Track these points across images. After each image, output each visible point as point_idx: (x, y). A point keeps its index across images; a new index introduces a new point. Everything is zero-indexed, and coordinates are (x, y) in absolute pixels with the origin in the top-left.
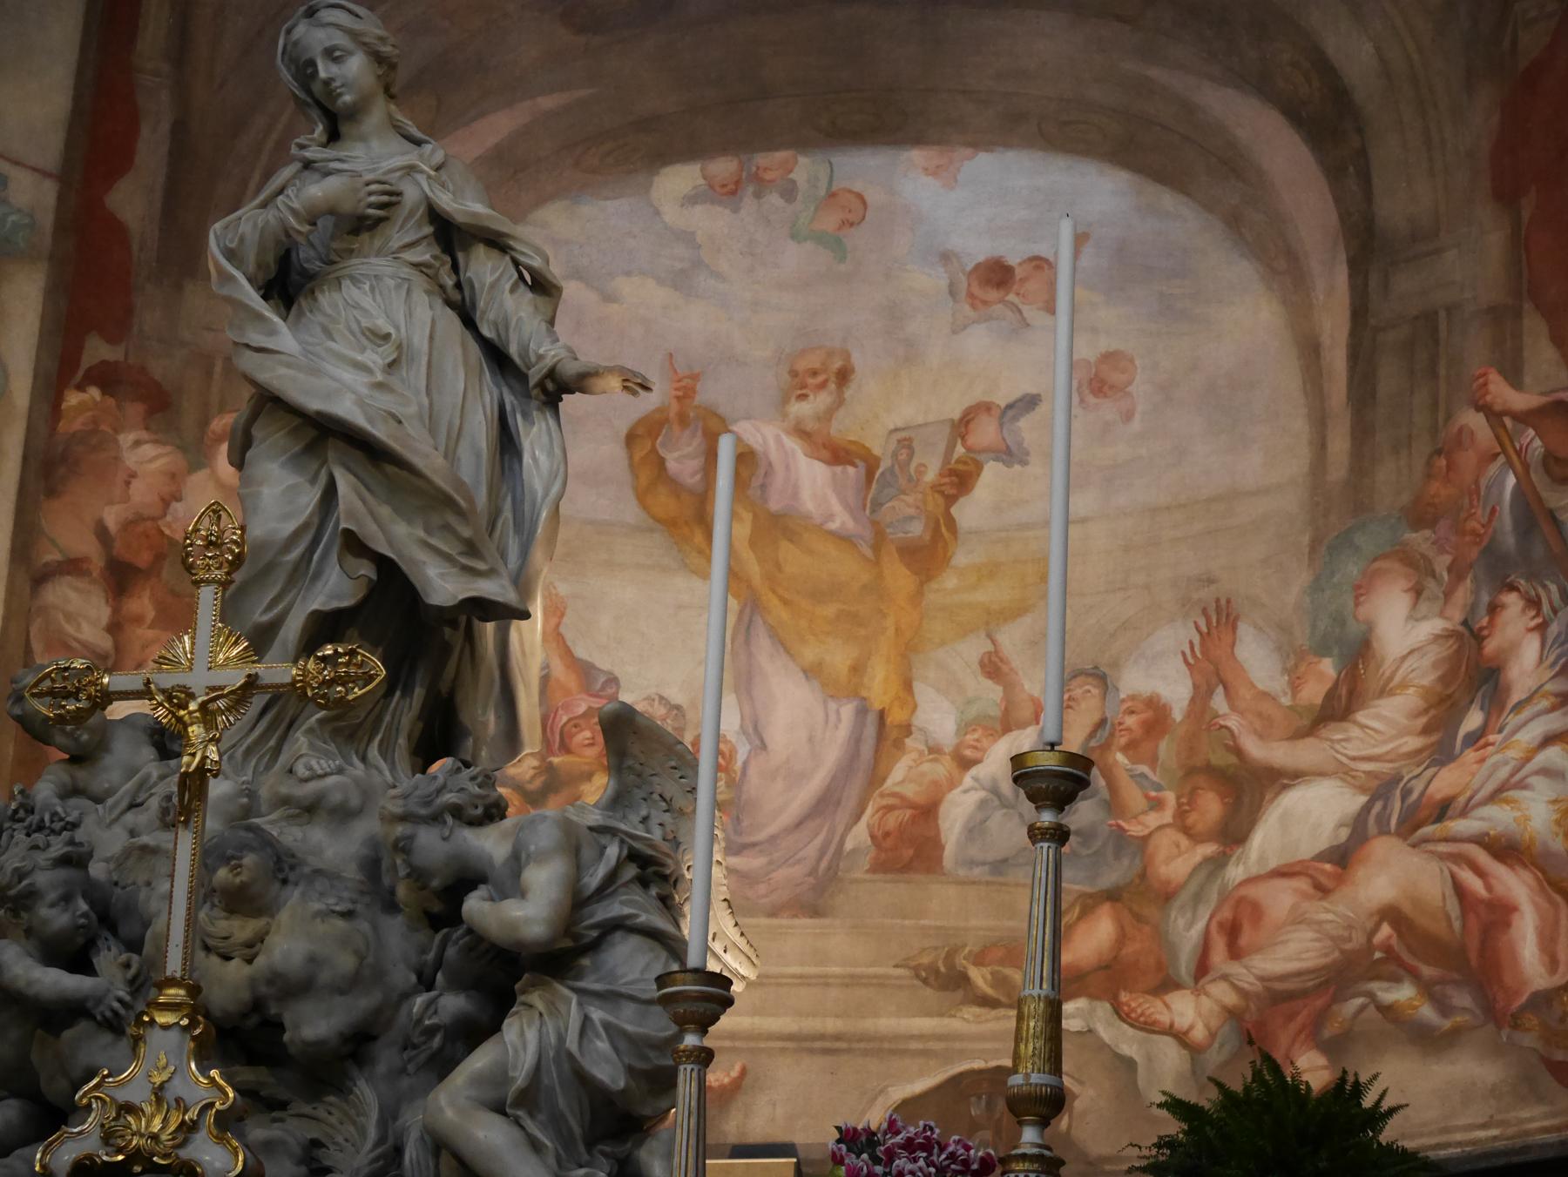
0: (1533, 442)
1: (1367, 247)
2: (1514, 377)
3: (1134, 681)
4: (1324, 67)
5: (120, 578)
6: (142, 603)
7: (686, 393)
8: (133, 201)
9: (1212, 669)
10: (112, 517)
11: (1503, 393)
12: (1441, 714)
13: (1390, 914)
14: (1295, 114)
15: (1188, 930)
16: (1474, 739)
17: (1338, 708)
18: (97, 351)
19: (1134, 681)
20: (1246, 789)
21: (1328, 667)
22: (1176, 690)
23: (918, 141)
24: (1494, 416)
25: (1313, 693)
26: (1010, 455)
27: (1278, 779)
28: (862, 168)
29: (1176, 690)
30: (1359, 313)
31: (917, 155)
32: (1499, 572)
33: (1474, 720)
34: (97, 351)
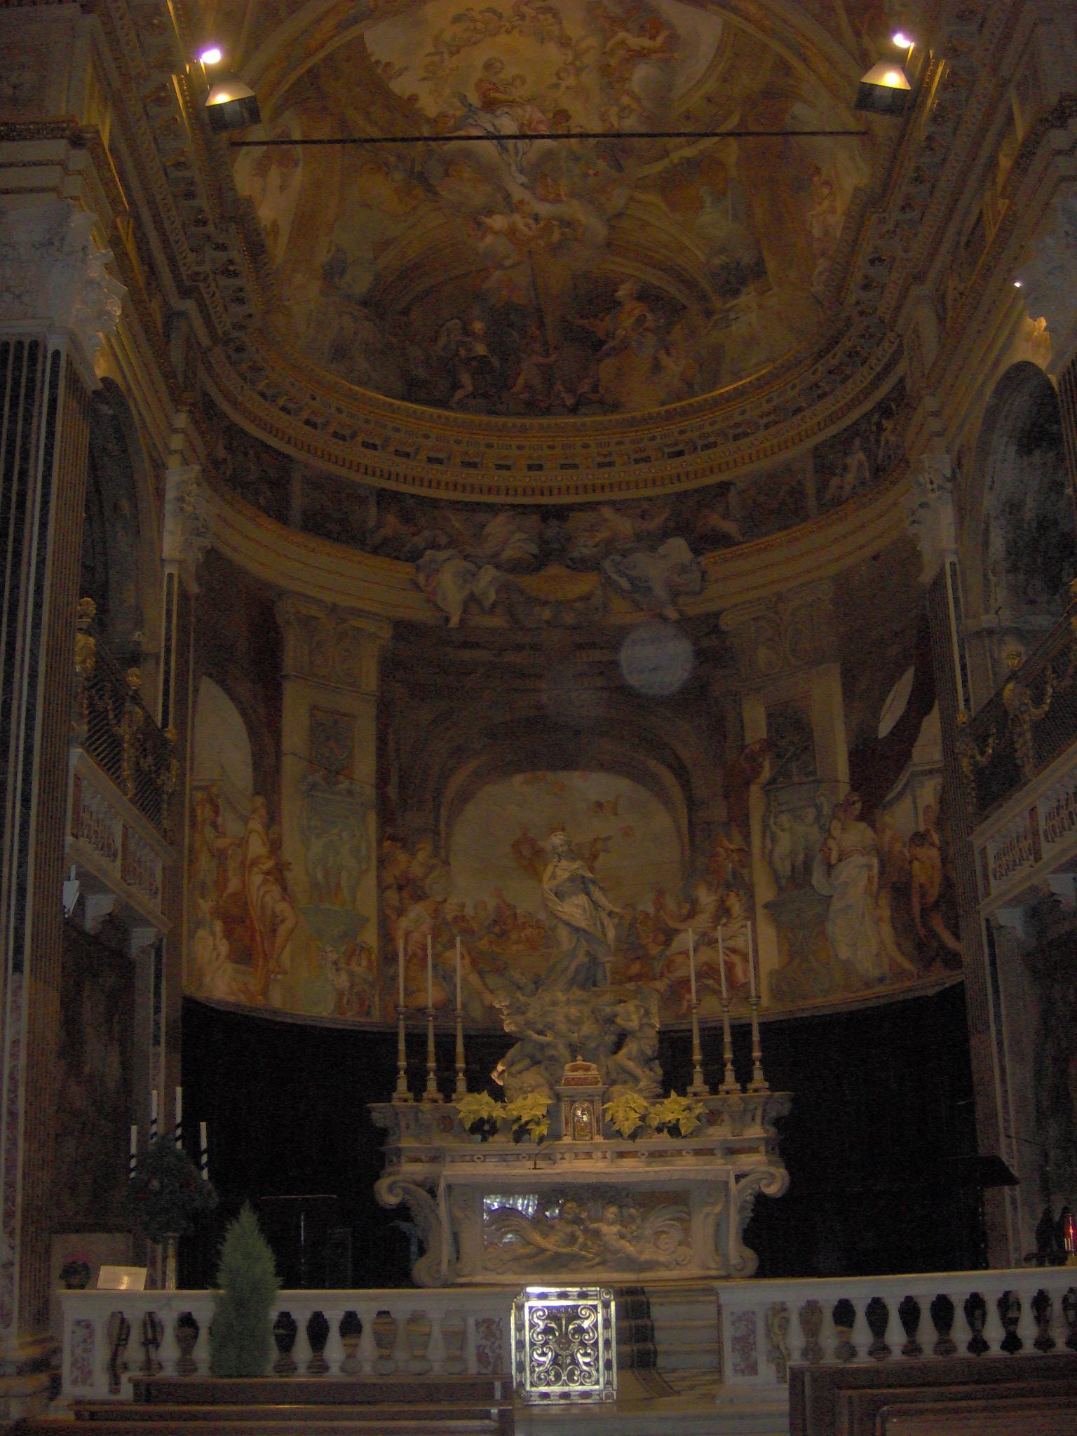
0: (735, 857)
1: (692, 804)
2: (730, 841)
3: (641, 907)
4: (677, 757)
5: (401, 888)
6: (405, 894)
7: (525, 835)
8: (392, 791)
9: (659, 906)
10: (397, 873)
11: (726, 843)
12: (716, 919)
13: (706, 963)
14: (670, 766)
15: (658, 966)
16: (724, 925)
17: (691, 915)
18: (390, 830)
19: (641, 907)
20: (670, 935)
21: (688, 906)
22: (651, 910)
23: (575, 769)
24: (726, 850)
25: (684, 911)
26: (607, 851)
27: (677, 931)
28: (563, 776)
29: (651, 910)
30: (690, 821)
31: (577, 773)
32: (728, 886)
33: (724, 920)
34: (390, 830)
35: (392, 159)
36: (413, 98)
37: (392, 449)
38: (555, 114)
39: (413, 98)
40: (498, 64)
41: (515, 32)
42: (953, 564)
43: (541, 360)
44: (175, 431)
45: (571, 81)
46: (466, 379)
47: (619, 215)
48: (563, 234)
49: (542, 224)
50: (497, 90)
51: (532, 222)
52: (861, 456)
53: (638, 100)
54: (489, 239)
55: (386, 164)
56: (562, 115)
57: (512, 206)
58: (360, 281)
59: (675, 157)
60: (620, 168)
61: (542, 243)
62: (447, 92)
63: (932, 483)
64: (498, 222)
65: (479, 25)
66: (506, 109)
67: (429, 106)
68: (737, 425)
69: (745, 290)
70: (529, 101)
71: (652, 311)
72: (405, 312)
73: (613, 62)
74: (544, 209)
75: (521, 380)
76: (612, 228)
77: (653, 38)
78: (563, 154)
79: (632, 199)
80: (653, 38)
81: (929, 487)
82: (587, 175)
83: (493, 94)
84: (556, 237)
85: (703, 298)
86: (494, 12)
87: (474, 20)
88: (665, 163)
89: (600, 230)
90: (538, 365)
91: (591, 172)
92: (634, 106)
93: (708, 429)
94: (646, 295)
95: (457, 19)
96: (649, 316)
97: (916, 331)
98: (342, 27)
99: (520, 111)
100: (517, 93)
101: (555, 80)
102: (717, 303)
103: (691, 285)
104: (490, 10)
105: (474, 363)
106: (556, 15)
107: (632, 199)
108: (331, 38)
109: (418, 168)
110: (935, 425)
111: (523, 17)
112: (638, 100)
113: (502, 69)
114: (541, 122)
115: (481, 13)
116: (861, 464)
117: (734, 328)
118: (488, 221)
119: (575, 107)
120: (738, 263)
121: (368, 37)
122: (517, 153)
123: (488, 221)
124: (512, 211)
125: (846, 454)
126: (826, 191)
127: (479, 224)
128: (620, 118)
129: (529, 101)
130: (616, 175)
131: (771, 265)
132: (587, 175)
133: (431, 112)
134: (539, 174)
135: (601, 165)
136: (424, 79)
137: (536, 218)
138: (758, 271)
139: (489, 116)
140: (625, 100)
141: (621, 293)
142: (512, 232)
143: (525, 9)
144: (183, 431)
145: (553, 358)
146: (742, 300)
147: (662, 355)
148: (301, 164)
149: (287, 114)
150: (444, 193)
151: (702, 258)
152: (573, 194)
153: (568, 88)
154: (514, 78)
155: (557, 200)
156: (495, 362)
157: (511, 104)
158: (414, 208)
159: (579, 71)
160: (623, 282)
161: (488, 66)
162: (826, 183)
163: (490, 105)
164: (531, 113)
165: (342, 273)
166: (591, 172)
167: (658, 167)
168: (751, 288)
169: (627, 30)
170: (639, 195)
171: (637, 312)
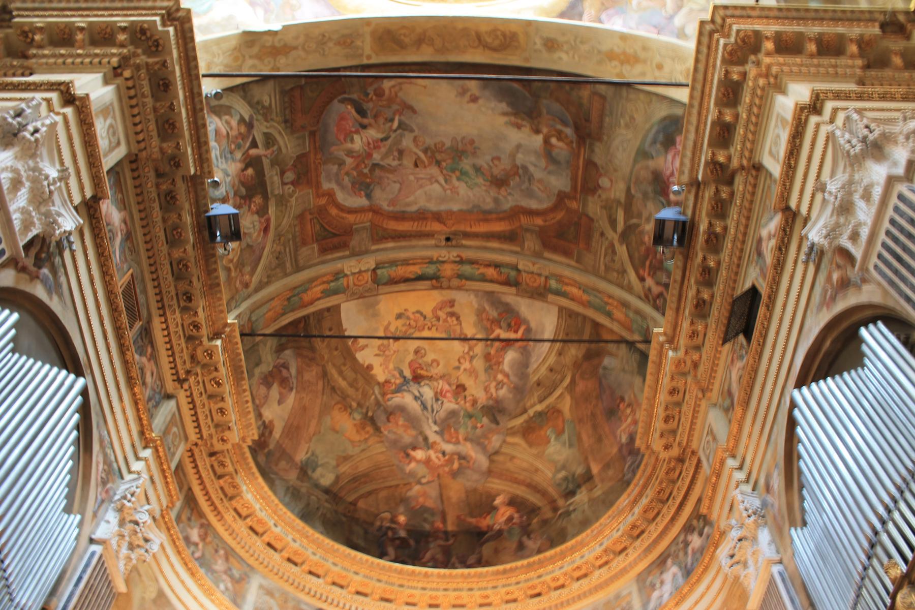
35: (354, 404)
36: (370, 367)
37: (329, 579)
38: (458, 386)
39: (370, 367)
40: (423, 351)
41: (434, 329)
42: (780, 574)
43: (442, 542)
44: (138, 458)
45: (466, 365)
46: (391, 551)
47: (497, 453)
48: (460, 464)
49: (447, 457)
50: (422, 369)
51: (440, 455)
52: (674, 569)
53: (507, 376)
54: (413, 465)
55: (351, 407)
56: (461, 388)
57: (427, 444)
58: (327, 480)
59: (531, 412)
60: (497, 423)
61: (447, 469)
62: (391, 366)
63: (746, 510)
64: (419, 454)
65: (412, 323)
66: (427, 382)
67: (380, 374)
68: (578, 568)
69: (579, 491)
70: (441, 377)
71: (518, 512)
72: (354, 504)
73: (493, 352)
74: (449, 448)
75: (428, 555)
76: (492, 461)
77: (516, 332)
78: (462, 413)
79: (504, 442)
80: (516, 332)
81: (745, 514)
82: (476, 428)
83: (419, 371)
84: (456, 465)
85: (553, 503)
86: (421, 314)
87: (408, 318)
88: (525, 417)
89: (482, 461)
90: (440, 546)
91: (479, 425)
92: (505, 380)
93: (557, 573)
94: (513, 502)
95: (399, 316)
96: (516, 515)
97: (711, 432)
98: (327, 293)
99: (435, 384)
100: (435, 371)
101: (457, 364)
102: (561, 502)
103: (543, 493)
104: (418, 312)
105: (398, 542)
106: (458, 318)
107: (504, 442)
108: (319, 299)
109: (370, 414)
110: (740, 476)
111: (438, 319)
112: (507, 376)
113: (425, 354)
114: (447, 391)
115: (413, 313)
116: (674, 575)
117: (573, 516)
118: (413, 453)
119: (469, 382)
120: (573, 476)
121: (343, 306)
122: (433, 411)
123: (413, 453)
124: (428, 449)
125: (661, 573)
126: (629, 411)
127: (408, 455)
128: (497, 390)
129: (441, 377)
130: (493, 426)
131: (595, 469)
132: (476, 428)
133: (381, 378)
134: (447, 425)
135: (485, 420)
136: (377, 355)
137: (444, 454)
138: (588, 477)
139: (416, 386)
140: (500, 377)
141: (498, 501)
142: (427, 462)
143: (441, 314)
144: (146, 460)
145: (451, 542)
146: (578, 498)
147: (525, 539)
148: (294, 391)
149: (288, 352)
150: (386, 433)
151: (550, 475)
152: (466, 439)
153: (465, 370)
154: (433, 361)
155: (457, 442)
156: (412, 542)
157: (431, 378)
158: (366, 440)
159: (472, 358)
160: (499, 495)
161: (417, 352)
162: (629, 405)
163: (417, 379)
164: (441, 385)
165: (314, 470)
166: (479, 425)
167: (519, 421)
168: (583, 489)
169: (501, 328)
170: (510, 439)
171: (508, 514)
